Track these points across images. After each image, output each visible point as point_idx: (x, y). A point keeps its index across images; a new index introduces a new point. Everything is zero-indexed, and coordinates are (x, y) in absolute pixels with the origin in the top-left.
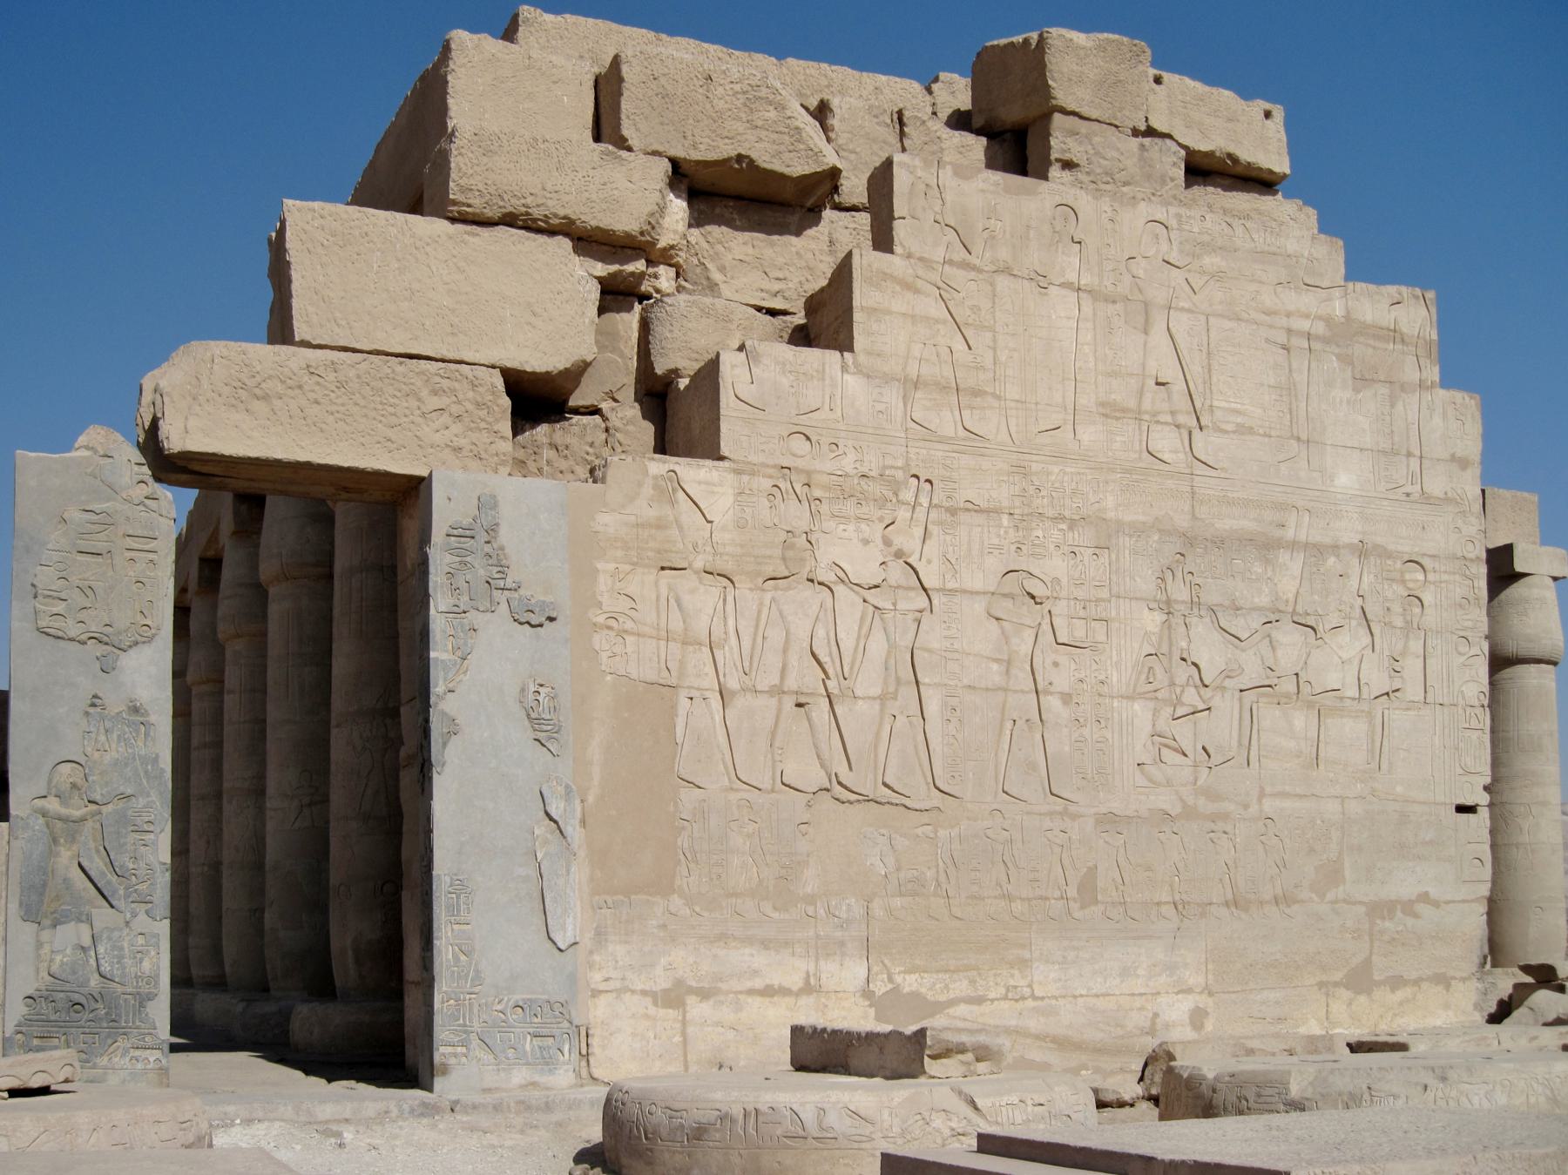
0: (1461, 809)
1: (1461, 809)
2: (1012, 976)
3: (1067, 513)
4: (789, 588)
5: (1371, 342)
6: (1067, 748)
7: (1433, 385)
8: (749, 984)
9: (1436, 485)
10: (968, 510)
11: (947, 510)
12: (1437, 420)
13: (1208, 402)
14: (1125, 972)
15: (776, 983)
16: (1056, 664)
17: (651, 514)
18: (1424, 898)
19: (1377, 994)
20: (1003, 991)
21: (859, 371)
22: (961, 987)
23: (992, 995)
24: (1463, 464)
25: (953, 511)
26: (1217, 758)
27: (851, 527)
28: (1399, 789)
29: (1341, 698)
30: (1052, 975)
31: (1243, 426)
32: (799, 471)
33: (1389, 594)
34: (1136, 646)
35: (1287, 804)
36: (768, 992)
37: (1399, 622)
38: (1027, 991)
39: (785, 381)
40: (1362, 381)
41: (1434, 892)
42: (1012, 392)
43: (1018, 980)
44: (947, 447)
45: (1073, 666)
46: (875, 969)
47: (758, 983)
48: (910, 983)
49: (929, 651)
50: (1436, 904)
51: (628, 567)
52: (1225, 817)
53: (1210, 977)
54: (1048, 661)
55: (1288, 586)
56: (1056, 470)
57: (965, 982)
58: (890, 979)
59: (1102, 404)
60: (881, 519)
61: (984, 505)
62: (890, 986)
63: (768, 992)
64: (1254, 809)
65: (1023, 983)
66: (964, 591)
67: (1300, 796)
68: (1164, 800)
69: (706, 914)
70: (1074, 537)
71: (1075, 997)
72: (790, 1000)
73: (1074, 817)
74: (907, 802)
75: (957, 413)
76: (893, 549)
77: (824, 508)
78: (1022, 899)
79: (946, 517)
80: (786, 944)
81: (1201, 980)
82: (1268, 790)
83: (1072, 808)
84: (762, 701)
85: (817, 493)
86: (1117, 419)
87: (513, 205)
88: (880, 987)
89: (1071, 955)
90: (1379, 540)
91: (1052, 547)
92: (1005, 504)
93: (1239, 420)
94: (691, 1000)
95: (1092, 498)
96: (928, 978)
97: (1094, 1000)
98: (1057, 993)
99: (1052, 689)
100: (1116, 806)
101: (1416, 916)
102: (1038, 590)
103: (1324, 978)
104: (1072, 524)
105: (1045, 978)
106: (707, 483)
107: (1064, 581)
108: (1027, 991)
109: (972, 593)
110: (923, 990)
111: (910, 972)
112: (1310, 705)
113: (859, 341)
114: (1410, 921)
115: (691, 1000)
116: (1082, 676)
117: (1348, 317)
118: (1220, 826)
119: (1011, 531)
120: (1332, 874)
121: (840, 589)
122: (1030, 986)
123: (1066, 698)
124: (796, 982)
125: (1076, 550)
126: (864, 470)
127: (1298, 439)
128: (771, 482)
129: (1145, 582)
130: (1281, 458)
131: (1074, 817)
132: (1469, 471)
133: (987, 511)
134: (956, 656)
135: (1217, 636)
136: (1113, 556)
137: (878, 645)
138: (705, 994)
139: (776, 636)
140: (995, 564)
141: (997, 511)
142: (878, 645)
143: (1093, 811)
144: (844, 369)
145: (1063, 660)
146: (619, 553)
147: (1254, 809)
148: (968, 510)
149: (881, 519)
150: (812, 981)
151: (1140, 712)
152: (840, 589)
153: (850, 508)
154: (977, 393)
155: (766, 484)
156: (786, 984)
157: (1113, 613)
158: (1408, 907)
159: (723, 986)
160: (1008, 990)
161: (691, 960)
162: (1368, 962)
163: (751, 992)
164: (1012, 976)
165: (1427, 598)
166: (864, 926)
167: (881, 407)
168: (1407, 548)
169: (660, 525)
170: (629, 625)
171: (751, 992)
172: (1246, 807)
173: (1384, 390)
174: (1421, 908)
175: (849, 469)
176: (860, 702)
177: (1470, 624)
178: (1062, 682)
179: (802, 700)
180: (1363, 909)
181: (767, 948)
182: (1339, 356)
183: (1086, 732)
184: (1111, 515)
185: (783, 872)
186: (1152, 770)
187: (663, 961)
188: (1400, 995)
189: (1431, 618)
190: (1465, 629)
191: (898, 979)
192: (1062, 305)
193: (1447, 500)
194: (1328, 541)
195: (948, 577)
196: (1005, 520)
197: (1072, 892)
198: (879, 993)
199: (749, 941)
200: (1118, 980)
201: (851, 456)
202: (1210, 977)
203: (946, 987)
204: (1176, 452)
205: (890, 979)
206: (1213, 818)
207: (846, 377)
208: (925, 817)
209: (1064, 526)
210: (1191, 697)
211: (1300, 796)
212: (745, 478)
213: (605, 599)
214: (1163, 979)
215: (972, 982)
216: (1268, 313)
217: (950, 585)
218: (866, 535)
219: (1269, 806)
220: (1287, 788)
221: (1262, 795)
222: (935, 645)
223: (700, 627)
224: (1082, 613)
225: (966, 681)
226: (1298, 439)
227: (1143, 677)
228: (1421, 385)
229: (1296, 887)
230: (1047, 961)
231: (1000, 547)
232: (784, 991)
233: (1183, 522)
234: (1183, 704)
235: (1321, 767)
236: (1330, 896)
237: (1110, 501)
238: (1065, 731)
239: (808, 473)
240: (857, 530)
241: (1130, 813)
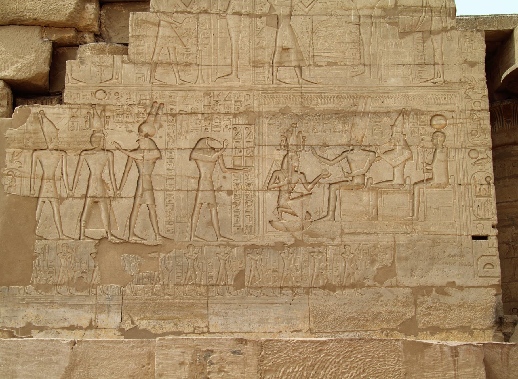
0: (475, 238)
1: (475, 238)
2: (197, 322)
3: (232, 111)
4: (93, 154)
5: (411, 14)
6: (230, 215)
7: (452, 28)
8: (62, 325)
10: (182, 114)
11: (171, 115)
12: (455, 45)
13: (311, 54)
14: (261, 321)
15: (75, 324)
16: (225, 178)
17: (32, 128)
18: (452, 284)
20: (192, 329)
21: (131, 62)
22: (169, 327)
23: (186, 331)
24: (472, 64)
25: (173, 115)
26: (314, 217)
27: (123, 127)
28: (432, 229)
29: (392, 185)
30: (220, 322)
31: (332, 62)
32: (99, 105)
33: (423, 132)
34: (269, 167)
35: (359, 238)
36: (72, 328)
37: (430, 145)
38: (205, 330)
39: (95, 69)
40: (404, 34)
41: (458, 282)
42: (204, 62)
43: (201, 324)
44: (171, 89)
45: (234, 178)
46: (125, 318)
47: (67, 324)
48: (144, 325)
49: (159, 175)
50: (461, 288)
51: (20, 150)
52: (320, 244)
53: (312, 324)
54: (221, 176)
55: (357, 134)
56: (227, 93)
57: (172, 325)
58: (133, 323)
59: (254, 62)
60: (138, 122)
61: (189, 111)
62: (132, 326)
63: (72, 328)
64: (338, 241)
65: (203, 325)
66: (178, 149)
67: (367, 234)
68: (285, 238)
69: (44, 293)
70: (238, 121)
71: (232, 333)
72: (82, 332)
73: (233, 246)
74: (145, 242)
75: (177, 74)
76: (143, 134)
77: (111, 120)
78: (204, 286)
79: (171, 118)
80: (82, 307)
81: (306, 326)
82: (346, 231)
83: (232, 243)
84: (76, 201)
85: (108, 113)
86: (260, 67)
87: (12, 16)
88: (127, 326)
89: (230, 312)
90: (415, 107)
91: (224, 126)
92: (200, 110)
93: (330, 60)
94: (34, 332)
95: (246, 103)
96: (152, 323)
97: (243, 334)
98: (222, 331)
99: (222, 189)
100: (257, 242)
101: (446, 294)
102: (217, 145)
103: (385, 326)
104: (235, 115)
105: (216, 323)
106: (58, 114)
107: (230, 141)
108: (205, 330)
109: (182, 149)
110: (149, 328)
111: (141, 319)
112: (373, 189)
113: (131, 49)
115: (34, 332)
116: (238, 182)
118: (316, 248)
119: (203, 121)
120: (388, 271)
121: (117, 153)
122: (207, 327)
123: (230, 193)
124: (85, 323)
125: (237, 126)
126: (131, 102)
127: (364, 65)
128: (86, 111)
129: (275, 137)
130: (354, 74)
131: (233, 246)
132: (476, 67)
133: (191, 114)
134: (172, 177)
135: (315, 159)
136: (257, 128)
137: (133, 174)
138: (41, 329)
139: (85, 174)
140: (194, 137)
141: (196, 114)
142: (133, 174)
143: (243, 243)
144: (123, 62)
145: (228, 175)
146: (17, 145)
147: (338, 241)
148: (182, 114)
149: (138, 122)
150: (93, 323)
151: (271, 197)
152: (117, 153)
153: (123, 119)
154: (187, 64)
155: (84, 112)
156: (80, 325)
157: (256, 153)
158: (442, 290)
159: (50, 326)
160: (195, 329)
161: (35, 314)
162: (413, 319)
163: (63, 328)
164: (197, 322)
165: (448, 131)
166: (121, 298)
167: (139, 75)
168: (433, 109)
169: (35, 133)
170: (18, 173)
171: (63, 328)
172: (333, 239)
173: (419, 35)
175: (124, 102)
176: (124, 199)
177: (478, 143)
178: (227, 186)
179: (97, 200)
180: (408, 290)
181: (72, 308)
182: (389, 24)
183: (240, 207)
184: (256, 110)
185: (82, 275)
186: (277, 224)
187: (22, 314)
189: (450, 141)
190: (476, 145)
191: (137, 323)
192: (232, 21)
194: (383, 110)
195: (170, 143)
196: (200, 117)
197: (230, 281)
198: (126, 329)
199: (64, 305)
200: (257, 325)
201: (125, 97)
202: (312, 324)
203: (162, 326)
204: (293, 78)
205: (133, 323)
206: (313, 245)
207: (124, 65)
208: (154, 249)
209: (231, 117)
210: (300, 188)
211: (367, 234)
212: (74, 111)
213: (8, 164)
214: (283, 325)
215: (176, 324)
216: (347, 10)
217: (170, 147)
218: (130, 129)
219: (346, 239)
220: (358, 230)
221: (342, 233)
222: (162, 173)
223: (48, 173)
224: (239, 154)
225: (177, 188)
226: (364, 65)
227: (272, 181)
228: (445, 30)
229: (365, 279)
230: (217, 315)
231: (196, 129)
232: (81, 328)
233: (296, 108)
234: (295, 192)
235: (380, 219)
236: (388, 282)
237: (255, 104)
238: (229, 207)
239: (104, 106)
240: (127, 127)
241: (263, 244)
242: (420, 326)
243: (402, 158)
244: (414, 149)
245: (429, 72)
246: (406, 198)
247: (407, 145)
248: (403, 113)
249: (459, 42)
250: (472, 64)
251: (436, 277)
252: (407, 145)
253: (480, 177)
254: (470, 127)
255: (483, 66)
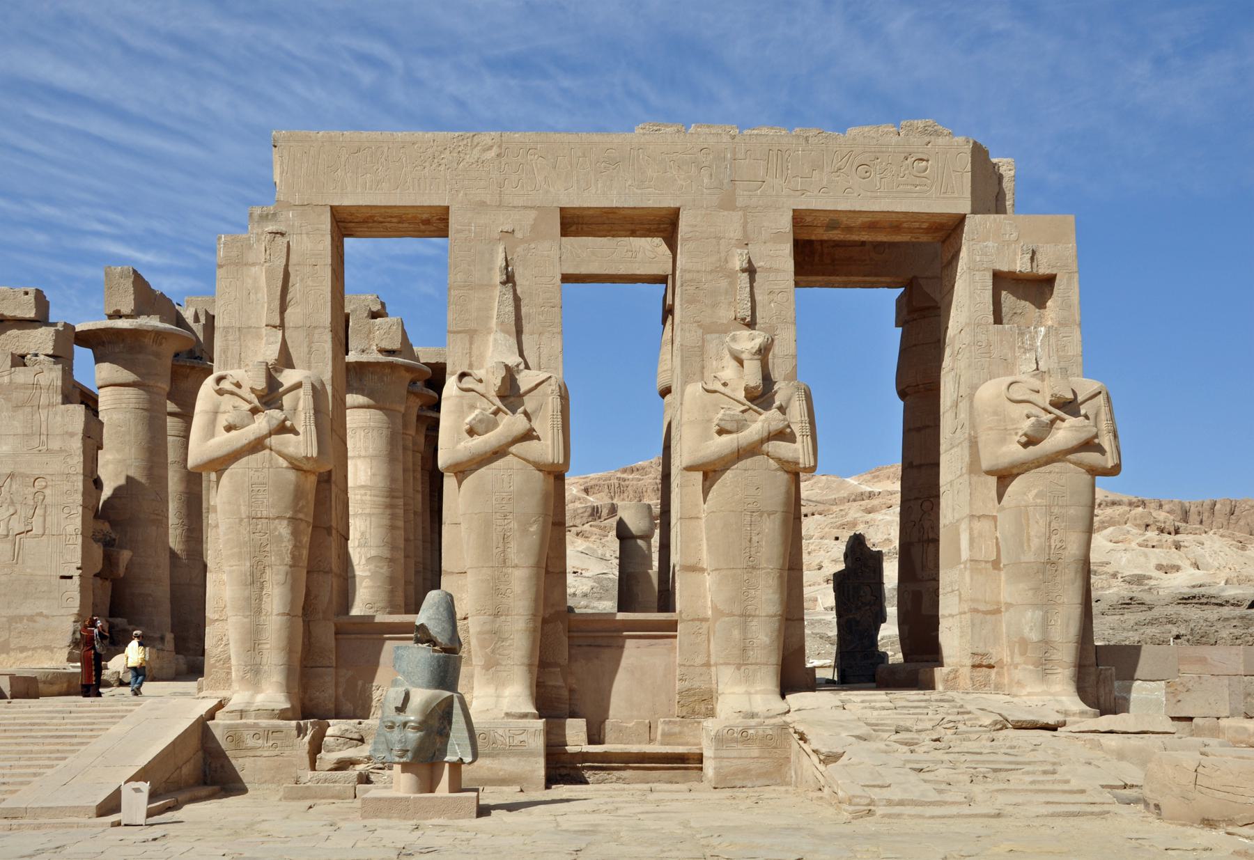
9: (55, 444)
12: (59, 418)
18: (41, 614)
19: (12, 654)
24: (72, 435)
41: (45, 612)
114: (31, 624)
117: (11, 383)
158: (31, 619)
165: (48, 492)
168: (37, 472)
174: (37, 618)
188: (25, 654)
189: (47, 501)
193: (61, 450)
242: (12, 646)
243: (8, 514)
244: (18, 507)
245: (35, 442)
246: (8, 546)
247: (12, 503)
248: (11, 476)
249: (63, 416)
250: (72, 435)
251: (27, 609)
252: (12, 503)
253: (70, 529)
254: (65, 488)
255: (80, 436)
